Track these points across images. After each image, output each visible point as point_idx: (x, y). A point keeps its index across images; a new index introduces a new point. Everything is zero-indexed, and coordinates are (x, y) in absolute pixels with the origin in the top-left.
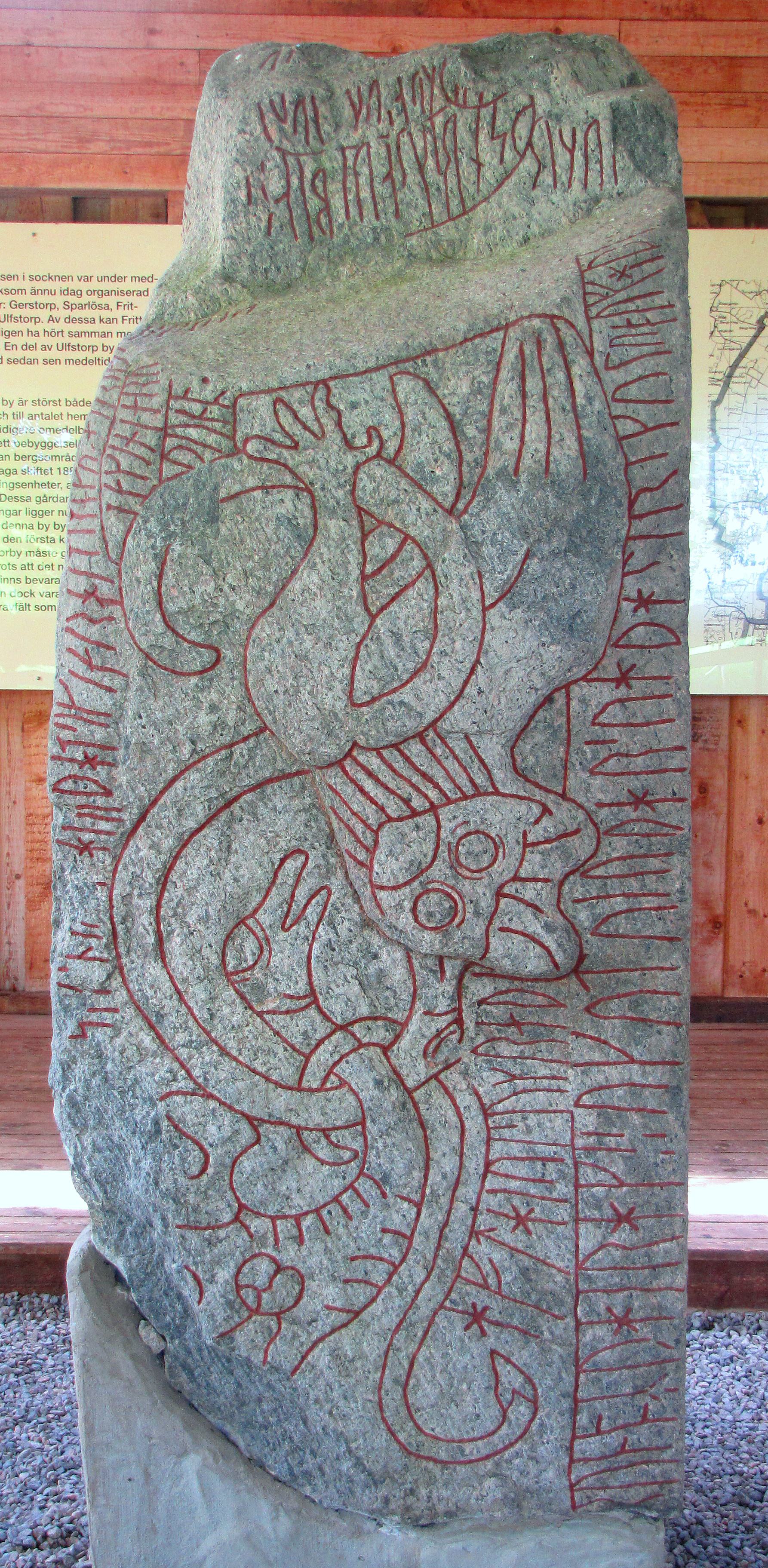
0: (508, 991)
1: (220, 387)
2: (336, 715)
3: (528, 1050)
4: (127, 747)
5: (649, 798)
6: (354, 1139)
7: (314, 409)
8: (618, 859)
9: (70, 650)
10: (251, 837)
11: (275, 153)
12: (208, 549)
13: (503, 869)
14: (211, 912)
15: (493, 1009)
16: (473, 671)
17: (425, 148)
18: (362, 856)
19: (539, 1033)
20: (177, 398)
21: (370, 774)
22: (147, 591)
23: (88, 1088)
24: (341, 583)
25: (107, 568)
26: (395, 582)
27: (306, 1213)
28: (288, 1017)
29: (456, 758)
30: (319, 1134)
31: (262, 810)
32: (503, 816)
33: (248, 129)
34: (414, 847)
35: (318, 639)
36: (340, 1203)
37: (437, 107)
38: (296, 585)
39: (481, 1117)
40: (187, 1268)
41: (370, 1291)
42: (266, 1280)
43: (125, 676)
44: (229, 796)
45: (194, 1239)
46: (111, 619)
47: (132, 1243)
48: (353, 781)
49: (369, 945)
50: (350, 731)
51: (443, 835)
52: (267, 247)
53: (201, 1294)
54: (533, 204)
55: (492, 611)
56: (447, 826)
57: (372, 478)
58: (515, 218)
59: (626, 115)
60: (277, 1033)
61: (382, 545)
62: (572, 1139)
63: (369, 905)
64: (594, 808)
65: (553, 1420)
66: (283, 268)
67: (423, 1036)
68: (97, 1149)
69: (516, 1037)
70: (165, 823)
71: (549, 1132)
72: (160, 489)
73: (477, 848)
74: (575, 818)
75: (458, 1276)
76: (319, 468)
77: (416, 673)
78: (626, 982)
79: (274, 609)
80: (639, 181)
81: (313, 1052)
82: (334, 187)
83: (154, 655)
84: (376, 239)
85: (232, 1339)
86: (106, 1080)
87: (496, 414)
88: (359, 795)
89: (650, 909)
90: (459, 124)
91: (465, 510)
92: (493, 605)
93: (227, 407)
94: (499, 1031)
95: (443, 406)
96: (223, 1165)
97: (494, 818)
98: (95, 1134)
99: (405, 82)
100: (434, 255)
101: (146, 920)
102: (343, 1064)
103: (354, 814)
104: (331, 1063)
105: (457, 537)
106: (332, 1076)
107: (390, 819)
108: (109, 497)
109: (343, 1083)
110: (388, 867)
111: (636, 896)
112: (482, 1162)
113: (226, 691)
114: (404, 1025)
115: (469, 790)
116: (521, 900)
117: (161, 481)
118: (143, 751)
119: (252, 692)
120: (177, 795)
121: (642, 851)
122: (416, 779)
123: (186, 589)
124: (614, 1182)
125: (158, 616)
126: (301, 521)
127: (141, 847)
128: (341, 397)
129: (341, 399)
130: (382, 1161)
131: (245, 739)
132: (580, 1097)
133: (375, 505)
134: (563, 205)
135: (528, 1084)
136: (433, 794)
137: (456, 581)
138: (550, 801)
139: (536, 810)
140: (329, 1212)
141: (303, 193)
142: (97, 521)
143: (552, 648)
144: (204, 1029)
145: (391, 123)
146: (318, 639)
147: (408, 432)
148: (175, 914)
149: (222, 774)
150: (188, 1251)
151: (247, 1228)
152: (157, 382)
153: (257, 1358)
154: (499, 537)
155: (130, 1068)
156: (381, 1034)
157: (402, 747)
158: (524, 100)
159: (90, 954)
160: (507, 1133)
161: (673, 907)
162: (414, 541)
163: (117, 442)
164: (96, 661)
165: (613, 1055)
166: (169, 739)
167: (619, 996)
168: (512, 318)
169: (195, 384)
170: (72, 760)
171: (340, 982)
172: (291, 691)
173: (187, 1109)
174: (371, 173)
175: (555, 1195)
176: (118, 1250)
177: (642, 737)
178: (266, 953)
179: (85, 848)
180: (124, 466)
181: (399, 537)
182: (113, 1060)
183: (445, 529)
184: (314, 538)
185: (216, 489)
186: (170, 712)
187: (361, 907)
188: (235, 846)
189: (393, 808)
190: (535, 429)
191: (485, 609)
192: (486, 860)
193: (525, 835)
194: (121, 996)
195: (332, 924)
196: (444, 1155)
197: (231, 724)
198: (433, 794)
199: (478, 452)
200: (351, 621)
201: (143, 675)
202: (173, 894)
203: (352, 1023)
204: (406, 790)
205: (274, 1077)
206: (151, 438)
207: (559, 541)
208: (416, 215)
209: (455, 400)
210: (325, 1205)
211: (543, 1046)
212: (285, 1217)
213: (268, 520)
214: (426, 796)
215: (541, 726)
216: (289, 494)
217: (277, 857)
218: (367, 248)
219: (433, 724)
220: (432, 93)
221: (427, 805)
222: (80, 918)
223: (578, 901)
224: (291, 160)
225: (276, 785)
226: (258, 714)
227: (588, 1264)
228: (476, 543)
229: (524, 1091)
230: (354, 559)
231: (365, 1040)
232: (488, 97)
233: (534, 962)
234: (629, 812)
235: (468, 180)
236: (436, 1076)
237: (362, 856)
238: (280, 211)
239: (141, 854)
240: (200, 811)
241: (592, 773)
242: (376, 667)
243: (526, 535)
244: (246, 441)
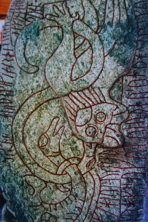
0: (107, 151)
1: (40, 2)
2: (67, 83)
3: (111, 165)
4: (16, 91)
5: (140, 104)
6: (69, 186)
7: (63, 8)
8: (134, 119)
9: (3, 68)
10: (46, 113)
12: (37, 42)
13: (107, 121)
14: (36, 132)
15: (103, 155)
16: (101, 72)
18: (73, 118)
19: (113, 161)
20: (29, 5)
21: (75, 98)
22: (21, 53)
23: (6, 173)
24: (69, 50)
25: (12, 47)
26: (82, 50)
27: (58, 203)
28: (54, 158)
29: (96, 94)
30: (61, 185)
31: (48, 107)
34: (86, 116)
35: (63, 64)
36: (65, 201)
38: (58, 51)
39: (99, 181)
40: (30, 215)
42: (48, 218)
43: (16, 74)
44: (40, 103)
45: (31, 209)
46: (13, 60)
47: (17, 209)
48: (71, 99)
49: (74, 140)
50: (71, 87)
51: (93, 113)
55: (106, 57)
56: (94, 111)
57: (77, 24)
60: (51, 161)
61: (79, 41)
62: (120, 186)
63: (74, 130)
64: (128, 106)
67: (86, 162)
68: (8, 187)
69: (108, 162)
70: (25, 110)
71: (115, 184)
72: (25, 28)
73: (101, 116)
74: (124, 109)
75: (93, 217)
76: (64, 22)
77: (87, 72)
78: (135, 148)
79: (53, 57)
81: (60, 166)
83: (23, 68)
86: (11, 171)
87: (107, 9)
88: (73, 103)
89: (140, 131)
91: (100, 32)
92: (106, 56)
93: (42, 7)
94: (104, 161)
95: (94, 7)
96: (38, 192)
97: (105, 109)
98: (8, 184)
101: (20, 134)
102: (67, 169)
103: (71, 108)
104: (64, 168)
105: (97, 39)
106: (64, 172)
107: (80, 109)
108: (14, 31)
109: (67, 173)
110: (80, 121)
111: (137, 128)
112: (99, 191)
113: (40, 78)
114: (82, 159)
115: (99, 102)
116: (111, 129)
117: (25, 26)
118: (20, 92)
119: (47, 77)
120: (28, 103)
121: (139, 117)
122: (87, 99)
123: (31, 52)
124: (130, 195)
125: (24, 59)
126: (59, 35)
127: (19, 116)
129: (69, 5)
130: (76, 191)
131: (45, 89)
132: (122, 176)
133: (78, 31)
135: (111, 173)
136: (91, 103)
137: (98, 49)
138: (118, 104)
139: (115, 107)
140: (63, 203)
142: (10, 36)
143: (120, 67)
144: (34, 160)
146: (63, 64)
147: (86, 13)
148: (27, 132)
149: (39, 98)
150: (30, 212)
151: (44, 207)
152: (25, 2)
154: (108, 39)
155: (16, 169)
157: (83, 91)
159: (7, 142)
160: (105, 185)
161: (146, 130)
162: (87, 40)
163: (15, 17)
164: (9, 70)
165: (131, 166)
166: (26, 89)
167: (133, 152)
170: (3, 95)
171: (67, 149)
172: (57, 77)
173: (30, 179)
175: (116, 199)
176: (14, 210)
178: (49, 142)
179: (6, 116)
180: (16, 22)
181: (83, 39)
182: (12, 167)
183: (95, 37)
184: (62, 39)
185: (39, 27)
186: (27, 82)
187: (72, 131)
188: (42, 116)
191: (104, 57)
192: (103, 119)
193: (112, 113)
194: (14, 152)
195: (65, 135)
196: (90, 190)
197: (41, 85)
198: (91, 103)
199: (103, 18)
200: (71, 59)
201: (20, 73)
202: (27, 127)
203: (69, 159)
204: (84, 102)
205: (51, 171)
206: (23, 16)
207: (122, 40)
209: (97, 5)
210: (62, 201)
211: (114, 164)
212: (52, 204)
213: (51, 34)
214: (89, 103)
215: (116, 86)
216: (56, 28)
217: (52, 118)
219: (91, 85)
221: (89, 105)
222: (5, 133)
223: (124, 129)
225: (52, 101)
226: (48, 83)
227: (123, 214)
228: (102, 40)
229: (110, 175)
230: (72, 44)
231: (72, 163)
233: (114, 144)
234: (136, 108)
236: (88, 171)
237: (73, 118)
239: (19, 118)
240: (34, 107)
241: (128, 98)
242: (77, 71)
243: (114, 38)
244: (46, 15)
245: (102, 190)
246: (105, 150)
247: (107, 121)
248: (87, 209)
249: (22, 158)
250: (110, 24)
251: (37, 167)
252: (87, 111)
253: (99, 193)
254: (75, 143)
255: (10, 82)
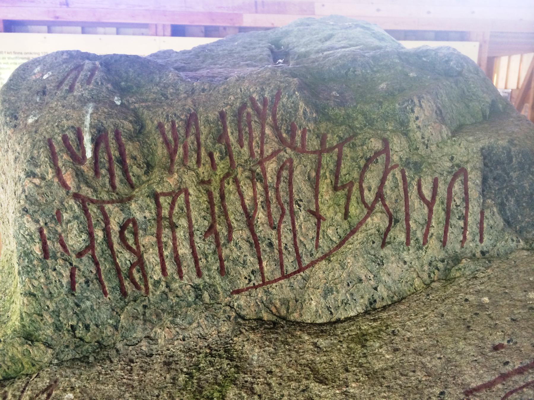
11: (72, 202)
17: (254, 199)
33: (37, 171)
37: (268, 150)
52: (72, 304)
58: (360, 281)
59: (499, 163)
66: (92, 327)
80: (510, 242)
82: (147, 240)
84: (199, 297)
90: (296, 172)
99: (229, 118)
100: (266, 316)
134: (416, 264)
141: (110, 246)
145: (214, 166)
158: (376, 145)
174: (190, 226)
208: (245, 273)
218: (189, 305)
220: (263, 133)
224: (93, 209)
232: (332, 140)
235: (306, 236)
238: (85, 265)
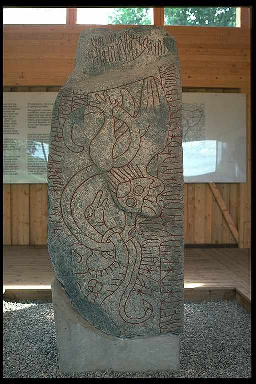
13: (145, 194)
19: (153, 230)
21: (117, 174)
24: (110, 132)
32: (145, 182)
38: (101, 133)
41: (117, 287)
51: (132, 186)
53: (81, 288)
54: (148, 58)
57: (117, 111)
60: (96, 231)
65: (157, 313)
85: (87, 298)
109: (111, 241)
110: (121, 194)
114: (124, 229)
122: (126, 175)
128: (110, 94)
136: (130, 178)
138: (154, 179)
153: (93, 302)
156: (119, 231)
158: (146, 37)
164: (58, 150)
168: (146, 77)
169: (79, 91)
177: (173, 166)
179: (55, 191)
185: (84, 114)
189: (122, 181)
190: (151, 100)
192: (142, 191)
198: (130, 178)
199: (139, 105)
212: (98, 271)
224: (98, 50)
233: (151, 214)
245: (143, 257)
246: (145, 219)
247: (145, 194)
248: (130, 276)
249: (70, 228)
250: (146, 110)
251: (84, 236)
252: (127, 185)
253: (141, 260)
254: (118, 214)
255: (58, 160)
